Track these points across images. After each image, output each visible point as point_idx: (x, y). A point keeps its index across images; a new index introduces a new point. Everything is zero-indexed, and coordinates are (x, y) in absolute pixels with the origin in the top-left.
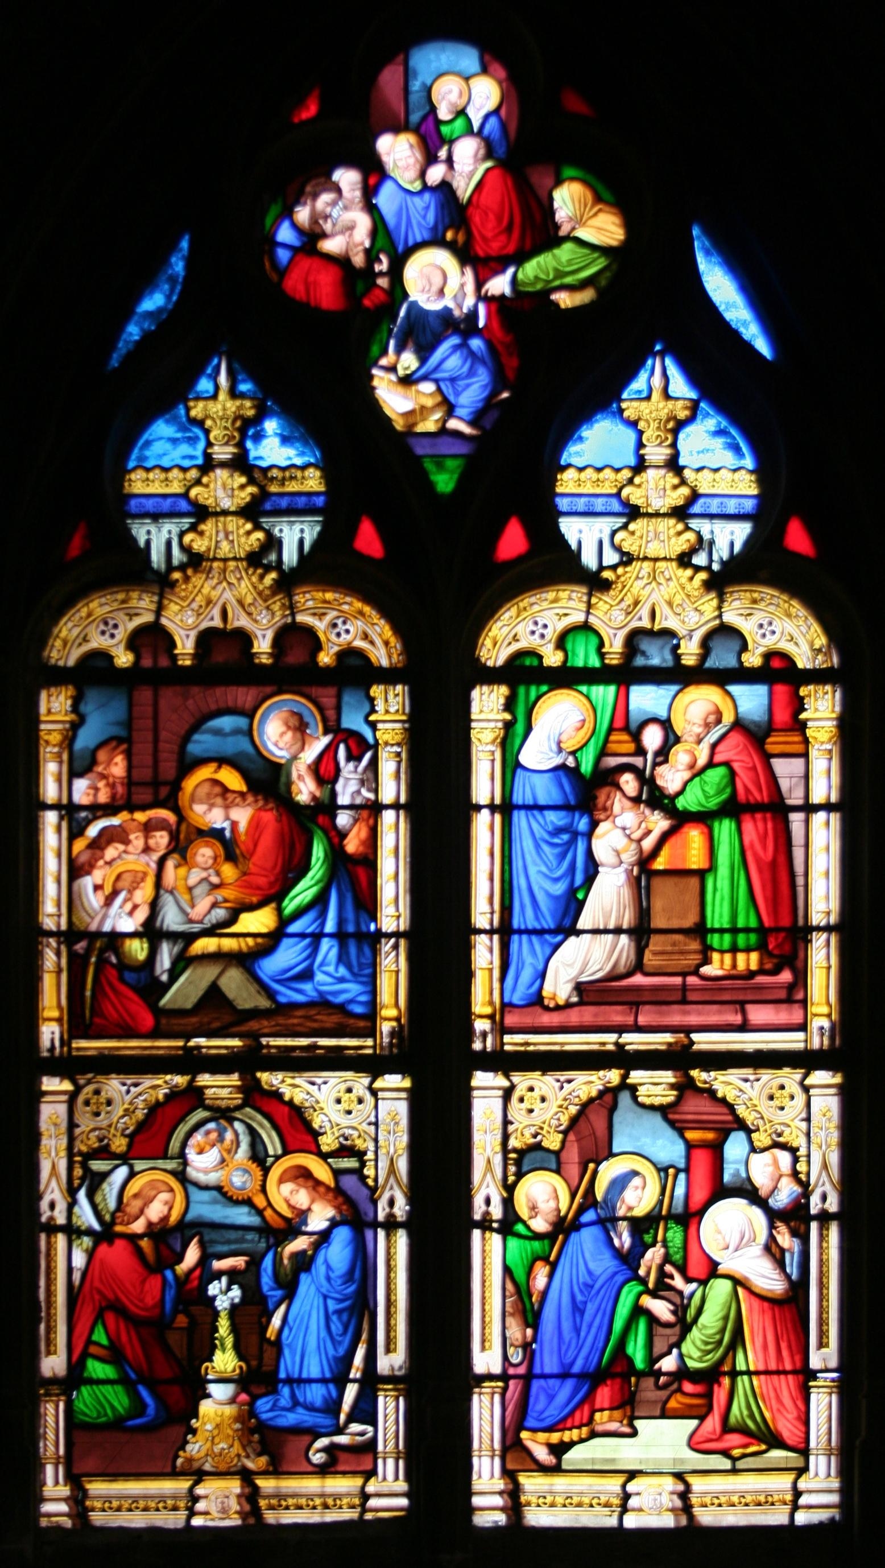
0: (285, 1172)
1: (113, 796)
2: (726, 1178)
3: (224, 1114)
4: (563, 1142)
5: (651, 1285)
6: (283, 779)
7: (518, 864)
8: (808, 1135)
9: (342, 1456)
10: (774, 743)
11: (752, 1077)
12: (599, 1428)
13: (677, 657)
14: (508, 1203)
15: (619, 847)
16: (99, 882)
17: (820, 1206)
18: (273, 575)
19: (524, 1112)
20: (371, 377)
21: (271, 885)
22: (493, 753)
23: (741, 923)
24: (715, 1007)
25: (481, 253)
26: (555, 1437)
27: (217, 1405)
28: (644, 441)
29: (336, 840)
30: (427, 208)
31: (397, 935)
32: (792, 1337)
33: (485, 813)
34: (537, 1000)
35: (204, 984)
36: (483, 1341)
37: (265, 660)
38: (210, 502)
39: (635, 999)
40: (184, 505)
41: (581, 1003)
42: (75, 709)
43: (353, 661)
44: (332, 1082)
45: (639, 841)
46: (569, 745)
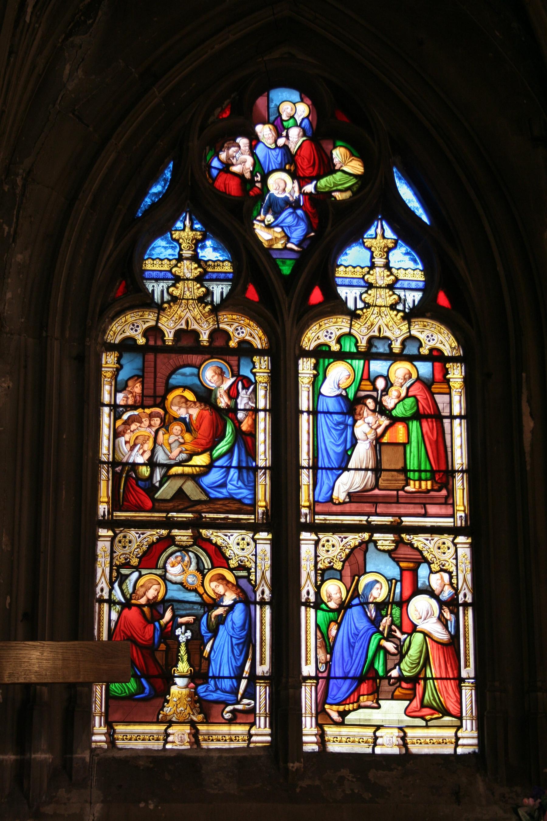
0: (212, 576)
1: (135, 401)
2: (419, 585)
3: (184, 549)
4: (343, 566)
5: (385, 635)
6: (213, 396)
7: (320, 438)
8: (457, 566)
9: (239, 715)
10: (435, 388)
11: (430, 538)
12: (362, 704)
13: (391, 349)
14: (318, 594)
15: (367, 432)
16: (128, 440)
17: (463, 599)
18: (210, 307)
19: (324, 552)
20: (254, 224)
21: (207, 443)
22: (309, 388)
23: (423, 468)
24: (412, 505)
25: (301, 175)
26: (341, 708)
27: (179, 689)
28: (374, 256)
29: (237, 425)
30: (278, 155)
31: (265, 468)
32: (452, 662)
33: (305, 414)
34: (330, 500)
35: (176, 488)
36: (306, 660)
37: (205, 344)
38: (181, 274)
39: (375, 501)
40: (169, 275)
41: (350, 502)
42: (118, 362)
43: (245, 346)
44: (235, 535)
45: (376, 429)
46: (343, 386)
